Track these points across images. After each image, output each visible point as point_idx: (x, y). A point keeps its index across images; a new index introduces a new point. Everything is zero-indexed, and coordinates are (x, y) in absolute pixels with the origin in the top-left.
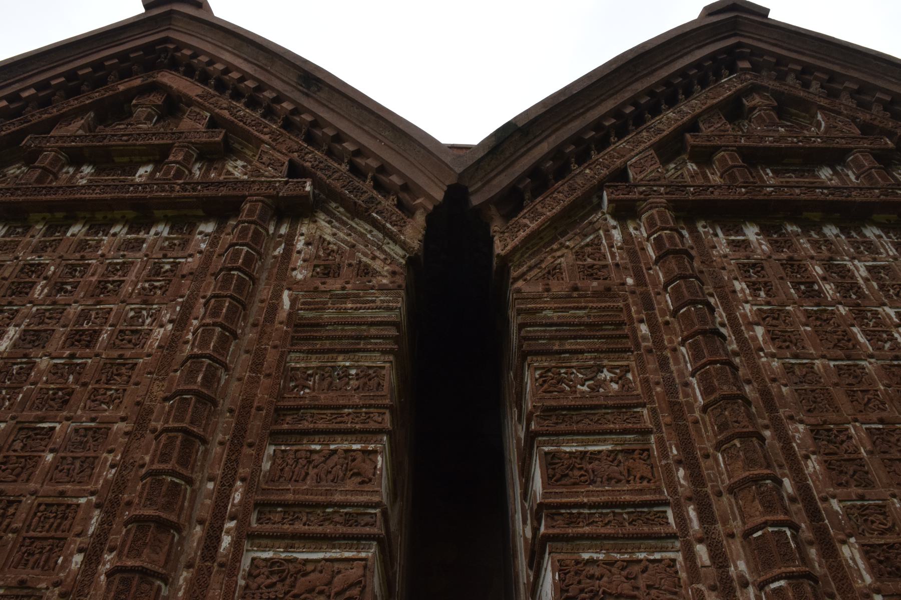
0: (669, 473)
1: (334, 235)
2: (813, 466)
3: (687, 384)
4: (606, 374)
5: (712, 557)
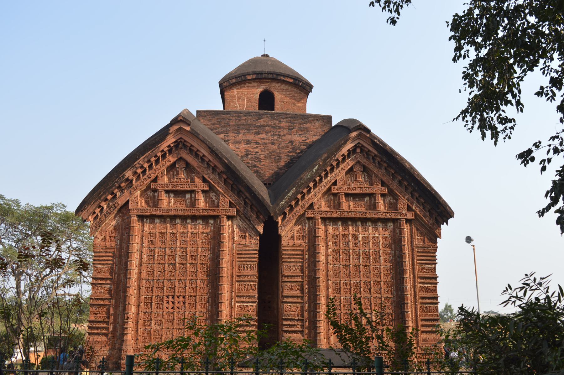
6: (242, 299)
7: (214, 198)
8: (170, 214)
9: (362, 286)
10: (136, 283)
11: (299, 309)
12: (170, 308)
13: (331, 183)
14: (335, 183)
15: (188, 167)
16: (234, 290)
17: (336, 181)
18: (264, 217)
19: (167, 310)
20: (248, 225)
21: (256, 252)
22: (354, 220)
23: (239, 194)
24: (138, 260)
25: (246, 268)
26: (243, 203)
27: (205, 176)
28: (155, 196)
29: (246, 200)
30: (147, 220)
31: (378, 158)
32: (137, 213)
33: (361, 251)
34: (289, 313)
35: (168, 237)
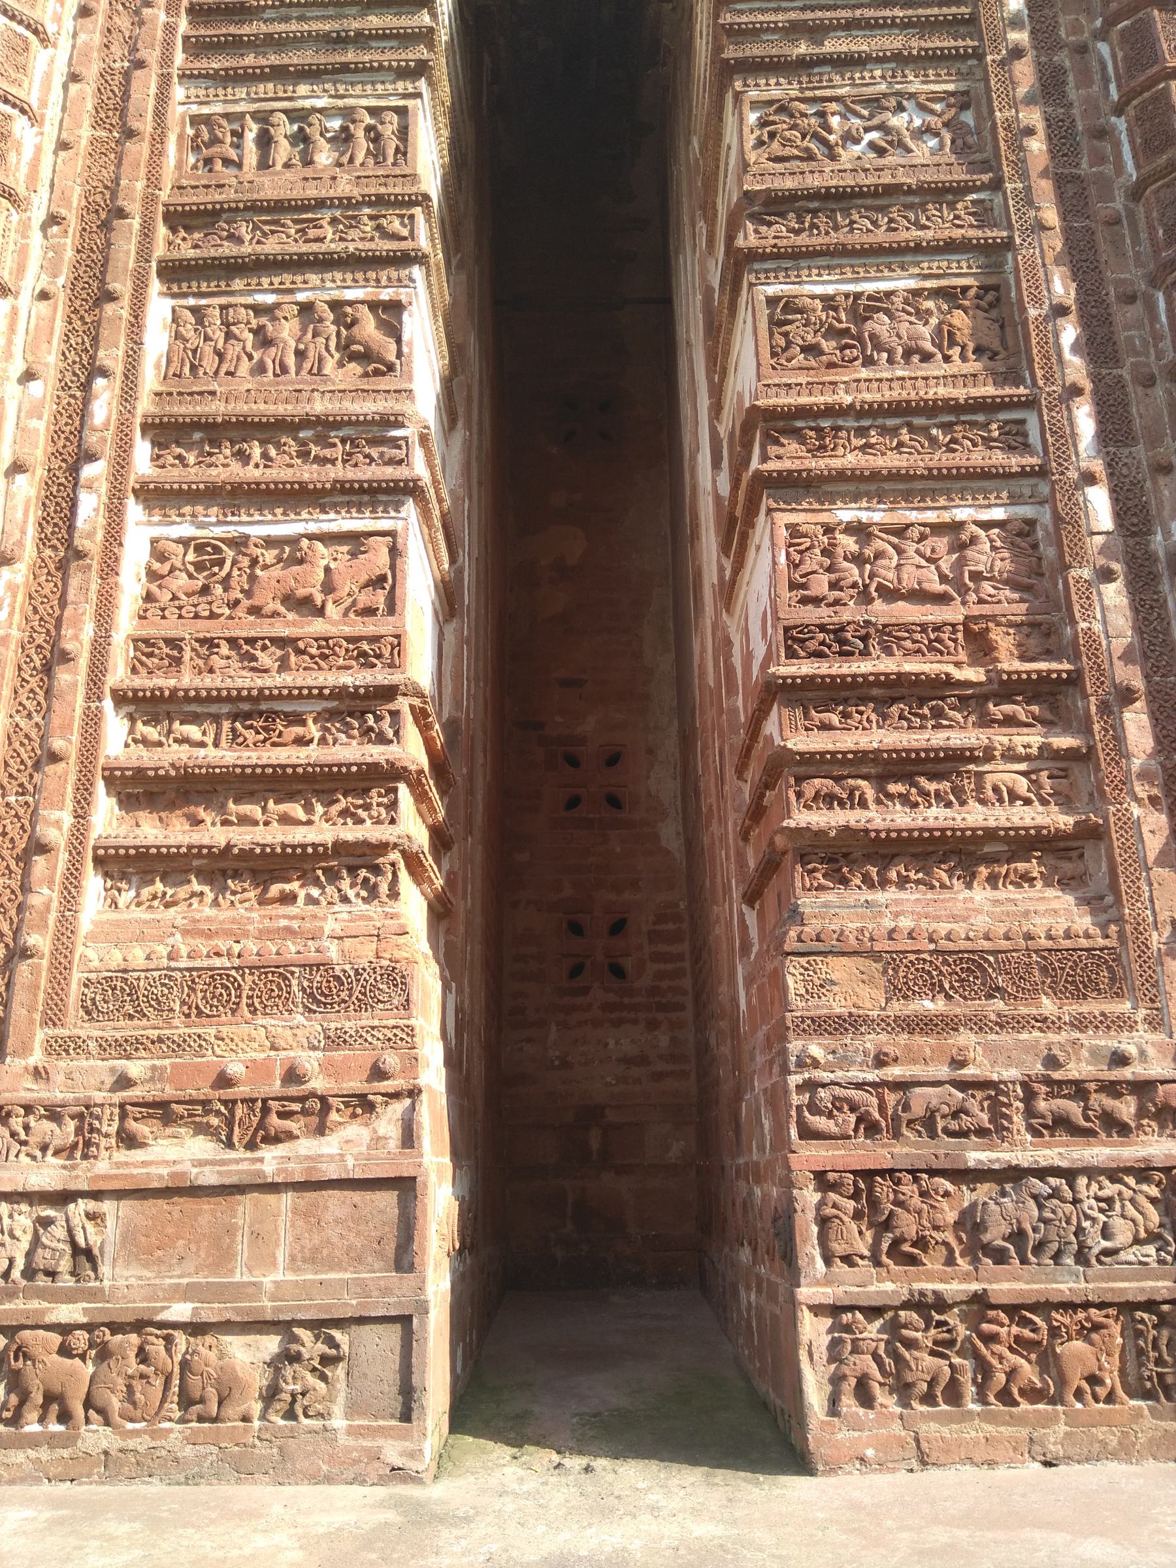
3: (1102, 133)
5: (1119, 515)
6: (226, 469)
11: (987, 556)
16: (112, 356)
25: (283, 150)
34: (850, 613)
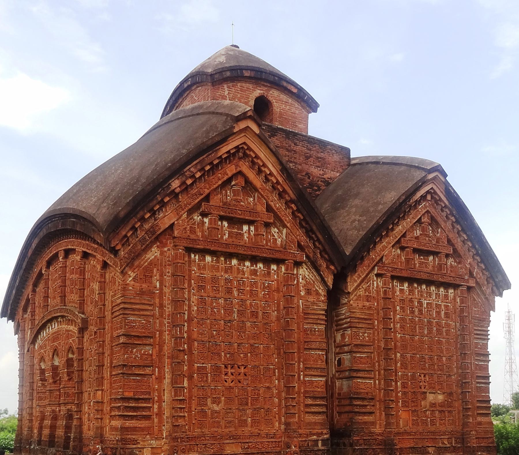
0: (374, 364)
1: (309, 276)
2: (399, 365)
4: (366, 335)
7: (276, 235)
8: (228, 250)
9: (427, 361)
10: (186, 346)
12: (230, 380)
13: (402, 234)
14: (404, 235)
15: (249, 187)
17: (406, 232)
18: (336, 268)
19: (227, 384)
20: (315, 276)
21: (323, 312)
22: (420, 282)
23: (309, 232)
24: (186, 312)
26: (313, 247)
27: (270, 203)
28: (203, 223)
29: (317, 244)
30: (195, 256)
31: (447, 210)
32: (186, 245)
33: (426, 320)
35: (222, 283)
